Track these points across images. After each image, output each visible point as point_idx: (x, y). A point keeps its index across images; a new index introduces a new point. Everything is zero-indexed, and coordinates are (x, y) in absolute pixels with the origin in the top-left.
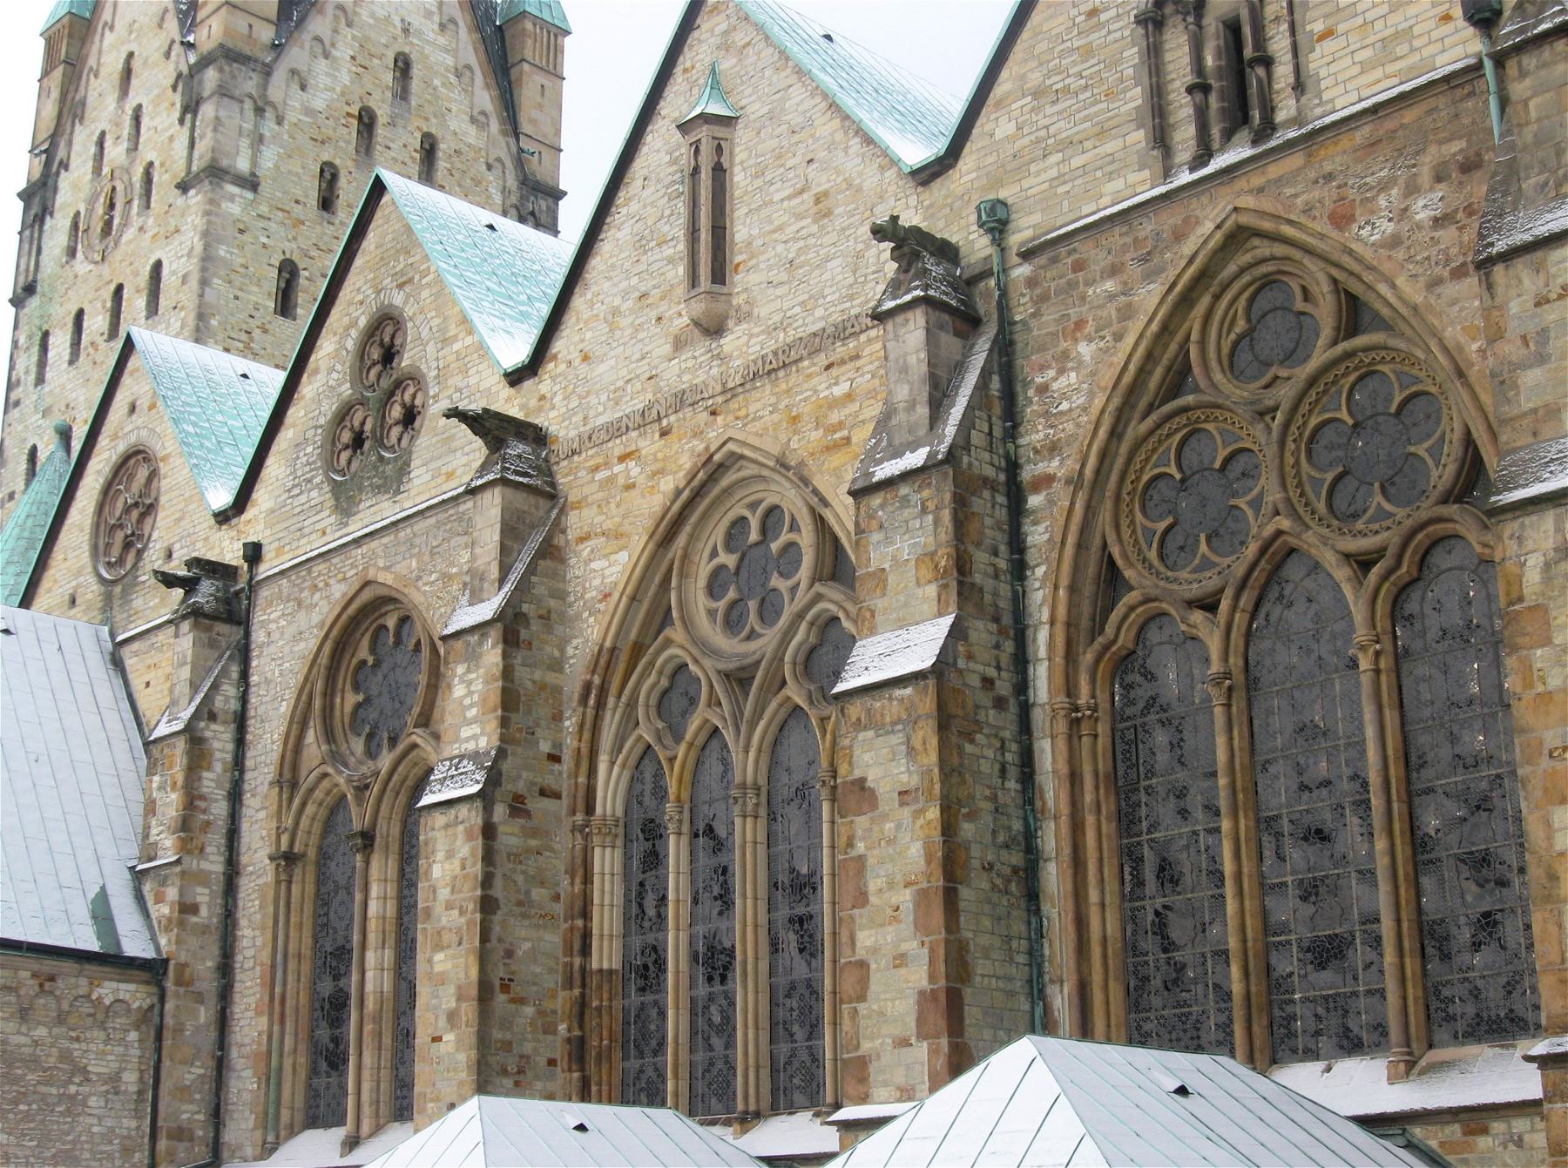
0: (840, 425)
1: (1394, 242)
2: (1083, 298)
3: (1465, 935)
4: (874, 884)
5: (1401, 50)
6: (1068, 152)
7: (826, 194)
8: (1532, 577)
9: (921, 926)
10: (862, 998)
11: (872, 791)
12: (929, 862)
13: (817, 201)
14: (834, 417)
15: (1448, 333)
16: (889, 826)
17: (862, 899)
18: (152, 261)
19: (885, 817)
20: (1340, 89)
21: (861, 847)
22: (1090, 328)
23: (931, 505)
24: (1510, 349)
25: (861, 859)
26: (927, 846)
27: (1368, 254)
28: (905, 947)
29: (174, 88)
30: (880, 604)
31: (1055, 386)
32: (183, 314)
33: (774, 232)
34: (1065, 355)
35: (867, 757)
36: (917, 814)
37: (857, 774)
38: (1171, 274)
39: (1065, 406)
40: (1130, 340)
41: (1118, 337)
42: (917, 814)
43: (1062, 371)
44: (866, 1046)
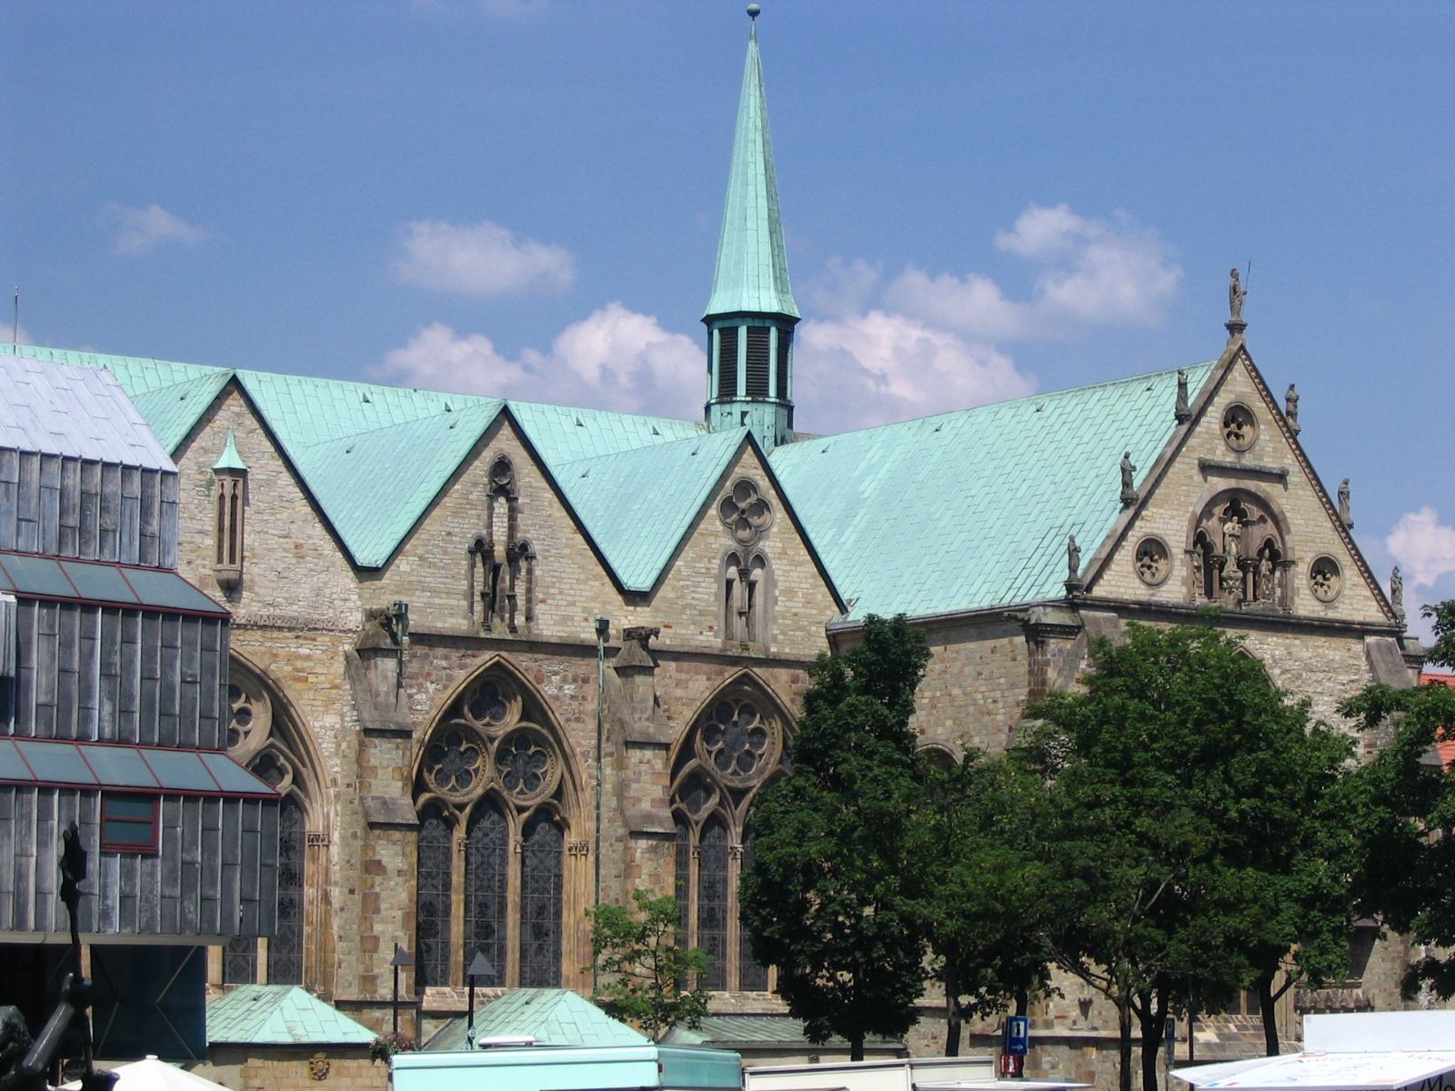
0: (302, 670)
1: (556, 698)
2: (432, 663)
3: (533, 953)
4: (383, 906)
5: (570, 623)
6: (434, 595)
7: (301, 545)
8: (638, 855)
9: (405, 926)
10: (376, 950)
11: (384, 867)
12: (410, 901)
13: (296, 547)
14: (299, 664)
15: (570, 740)
16: (392, 883)
17: (377, 910)
19: (390, 879)
20: (545, 627)
21: (377, 889)
22: (433, 677)
23: (401, 747)
24: (630, 773)
25: (377, 895)
26: (410, 895)
27: (547, 698)
28: (397, 934)
30: (374, 782)
31: (416, 697)
33: (269, 550)
34: (420, 686)
35: (383, 852)
36: (406, 881)
37: (377, 858)
38: (471, 670)
39: (419, 707)
40: (450, 691)
41: (445, 687)
42: (406, 881)
43: (419, 692)
44: (376, 971)
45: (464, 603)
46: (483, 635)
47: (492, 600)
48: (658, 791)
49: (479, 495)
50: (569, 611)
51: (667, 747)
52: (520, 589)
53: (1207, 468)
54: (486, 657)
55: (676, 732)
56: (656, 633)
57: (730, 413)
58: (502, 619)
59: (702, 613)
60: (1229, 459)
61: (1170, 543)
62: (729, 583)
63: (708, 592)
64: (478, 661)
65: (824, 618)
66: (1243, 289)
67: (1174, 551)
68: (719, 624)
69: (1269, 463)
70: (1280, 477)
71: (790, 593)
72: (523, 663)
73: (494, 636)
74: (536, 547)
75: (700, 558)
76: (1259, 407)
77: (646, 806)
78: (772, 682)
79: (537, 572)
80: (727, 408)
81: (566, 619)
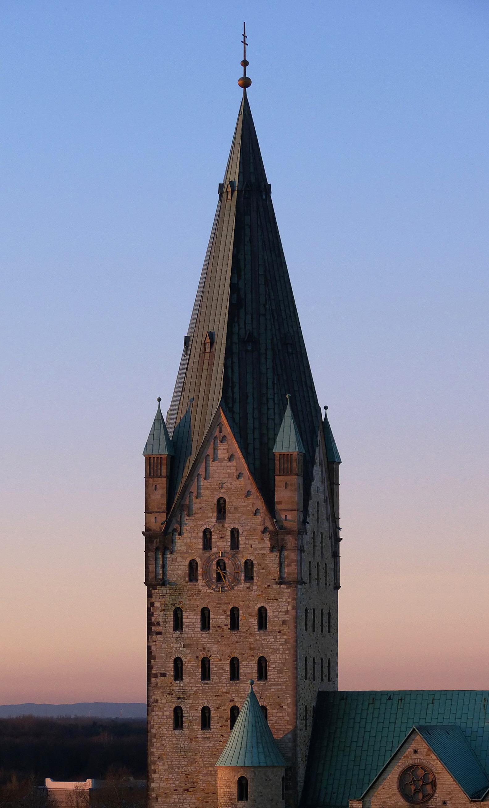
18: (259, 605)
29: (263, 532)
32: (285, 637)
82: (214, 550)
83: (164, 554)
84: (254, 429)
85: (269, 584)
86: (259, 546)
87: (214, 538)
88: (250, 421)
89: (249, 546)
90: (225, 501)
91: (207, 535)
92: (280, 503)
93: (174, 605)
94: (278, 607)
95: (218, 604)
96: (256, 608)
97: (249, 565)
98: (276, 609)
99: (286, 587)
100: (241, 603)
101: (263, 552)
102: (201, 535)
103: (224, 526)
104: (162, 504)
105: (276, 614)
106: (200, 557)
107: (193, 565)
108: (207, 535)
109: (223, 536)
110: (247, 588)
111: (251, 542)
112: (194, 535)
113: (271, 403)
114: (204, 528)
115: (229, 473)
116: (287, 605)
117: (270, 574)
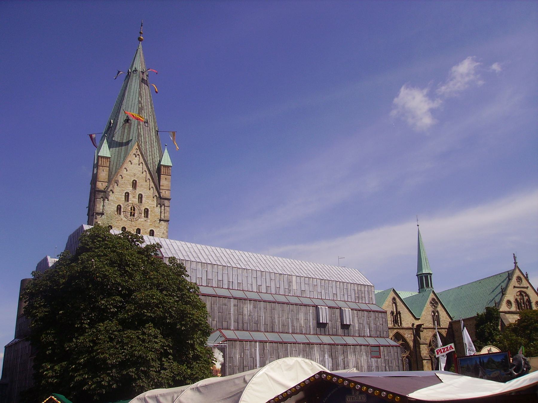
1: (407, 337)
8: (425, 363)
29: (153, 198)
45: (391, 322)
46: (394, 327)
47: (395, 321)
48: (427, 352)
49: (391, 304)
50: (408, 322)
51: (427, 344)
52: (399, 319)
53: (514, 287)
54: (395, 331)
55: (428, 342)
56: (423, 325)
57: (423, 290)
58: (397, 324)
59: (429, 321)
60: (519, 285)
61: (511, 301)
62: (433, 316)
63: (430, 318)
64: (394, 332)
65: (449, 321)
66: (516, 256)
67: (512, 302)
68: (432, 323)
69: (525, 286)
70: (527, 288)
71: (443, 317)
72: (401, 332)
73: (396, 327)
74: (401, 312)
75: (428, 312)
76: (522, 276)
77: (425, 355)
78: (442, 332)
79: (402, 316)
80: (423, 289)
81: (407, 324)
82: (130, 202)
83: (104, 200)
84: (150, 155)
85: (156, 220)
86: (152, 203)
87: (130, 196)
88: (148, 151)
89: (147, 202)
90: (136, 181)
91: (127, 195)
92: (163, 186)
93: (108, 224)
94: (159, 231)
95: (130, 226)
96: (149, 230)
97: (146, 211)
98: (158, 231)
99: (163, 222)
100: (142, 227)
101: (154, 206)
102: (124, 194)
103: (135, 192)
104: (106, 178)
105: (158, 234)
106: (123, 204)
107: (119, 208)
108: (127, 195)
109: (135, 196)
110: (145, 221)
111: (148, 201)
112: (121, 194)
113: (155, 147)
114: (126, 191)
115: (139, 170)
116: (164, 230)
117: (155, 216)
